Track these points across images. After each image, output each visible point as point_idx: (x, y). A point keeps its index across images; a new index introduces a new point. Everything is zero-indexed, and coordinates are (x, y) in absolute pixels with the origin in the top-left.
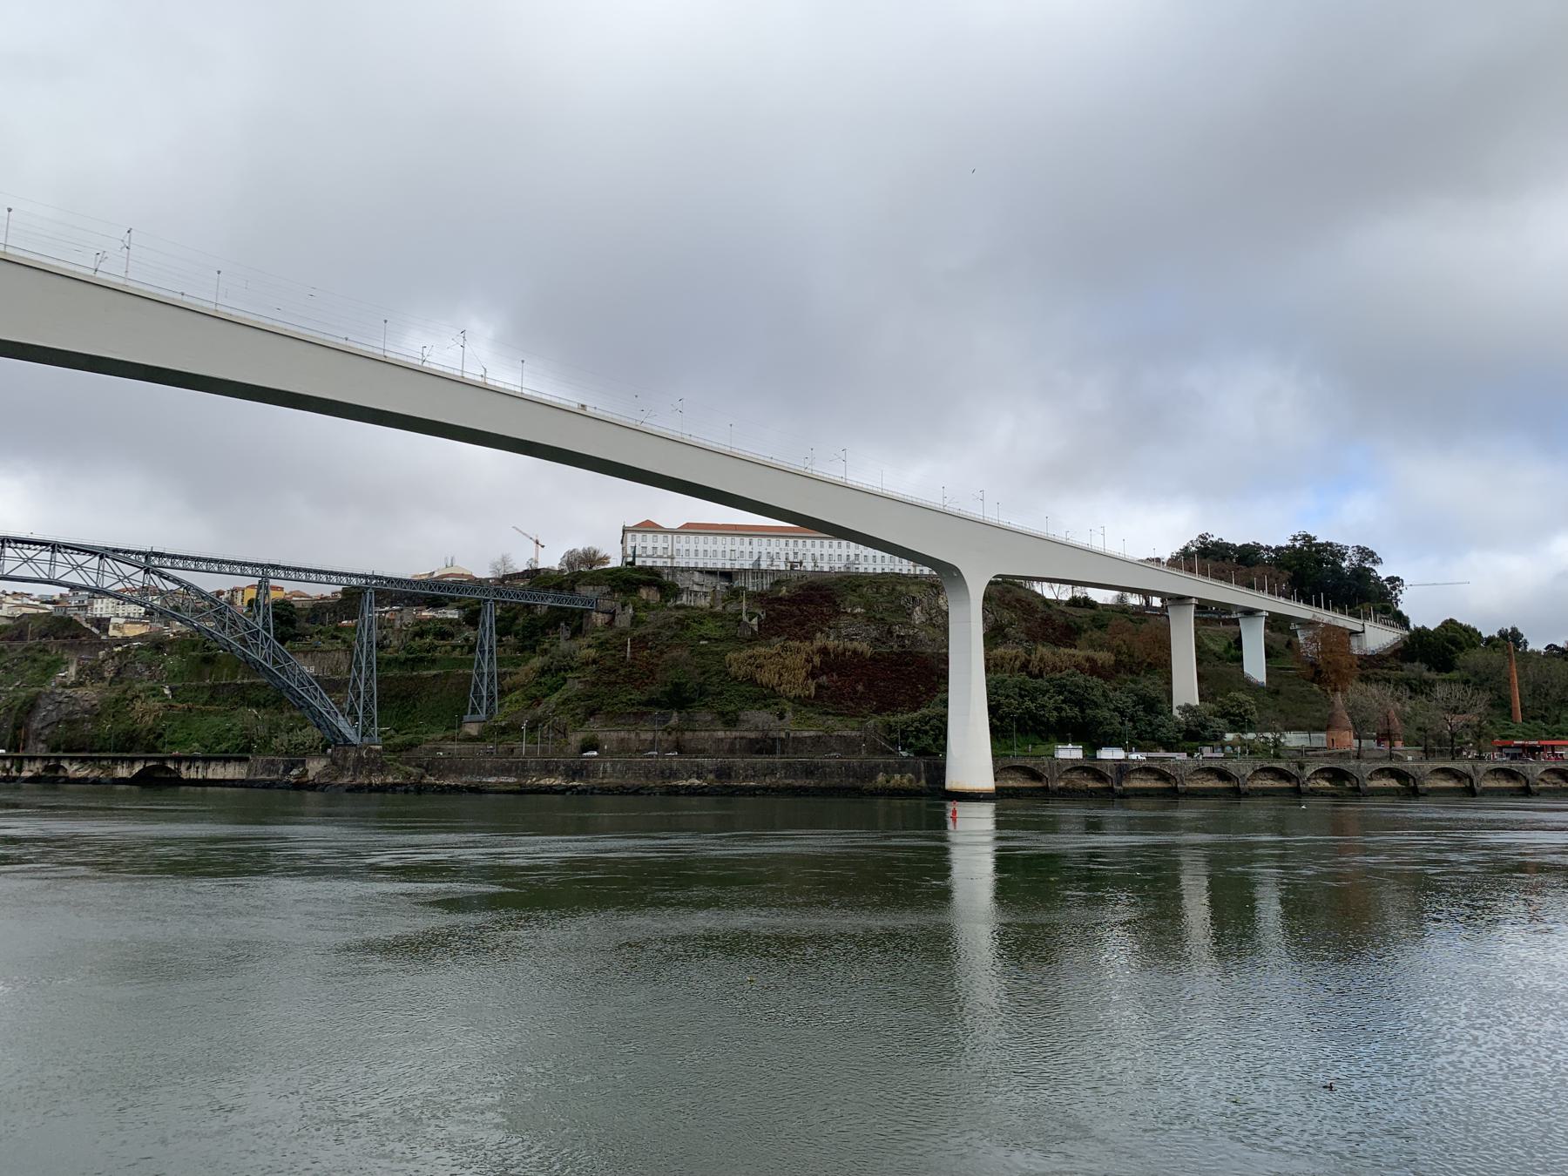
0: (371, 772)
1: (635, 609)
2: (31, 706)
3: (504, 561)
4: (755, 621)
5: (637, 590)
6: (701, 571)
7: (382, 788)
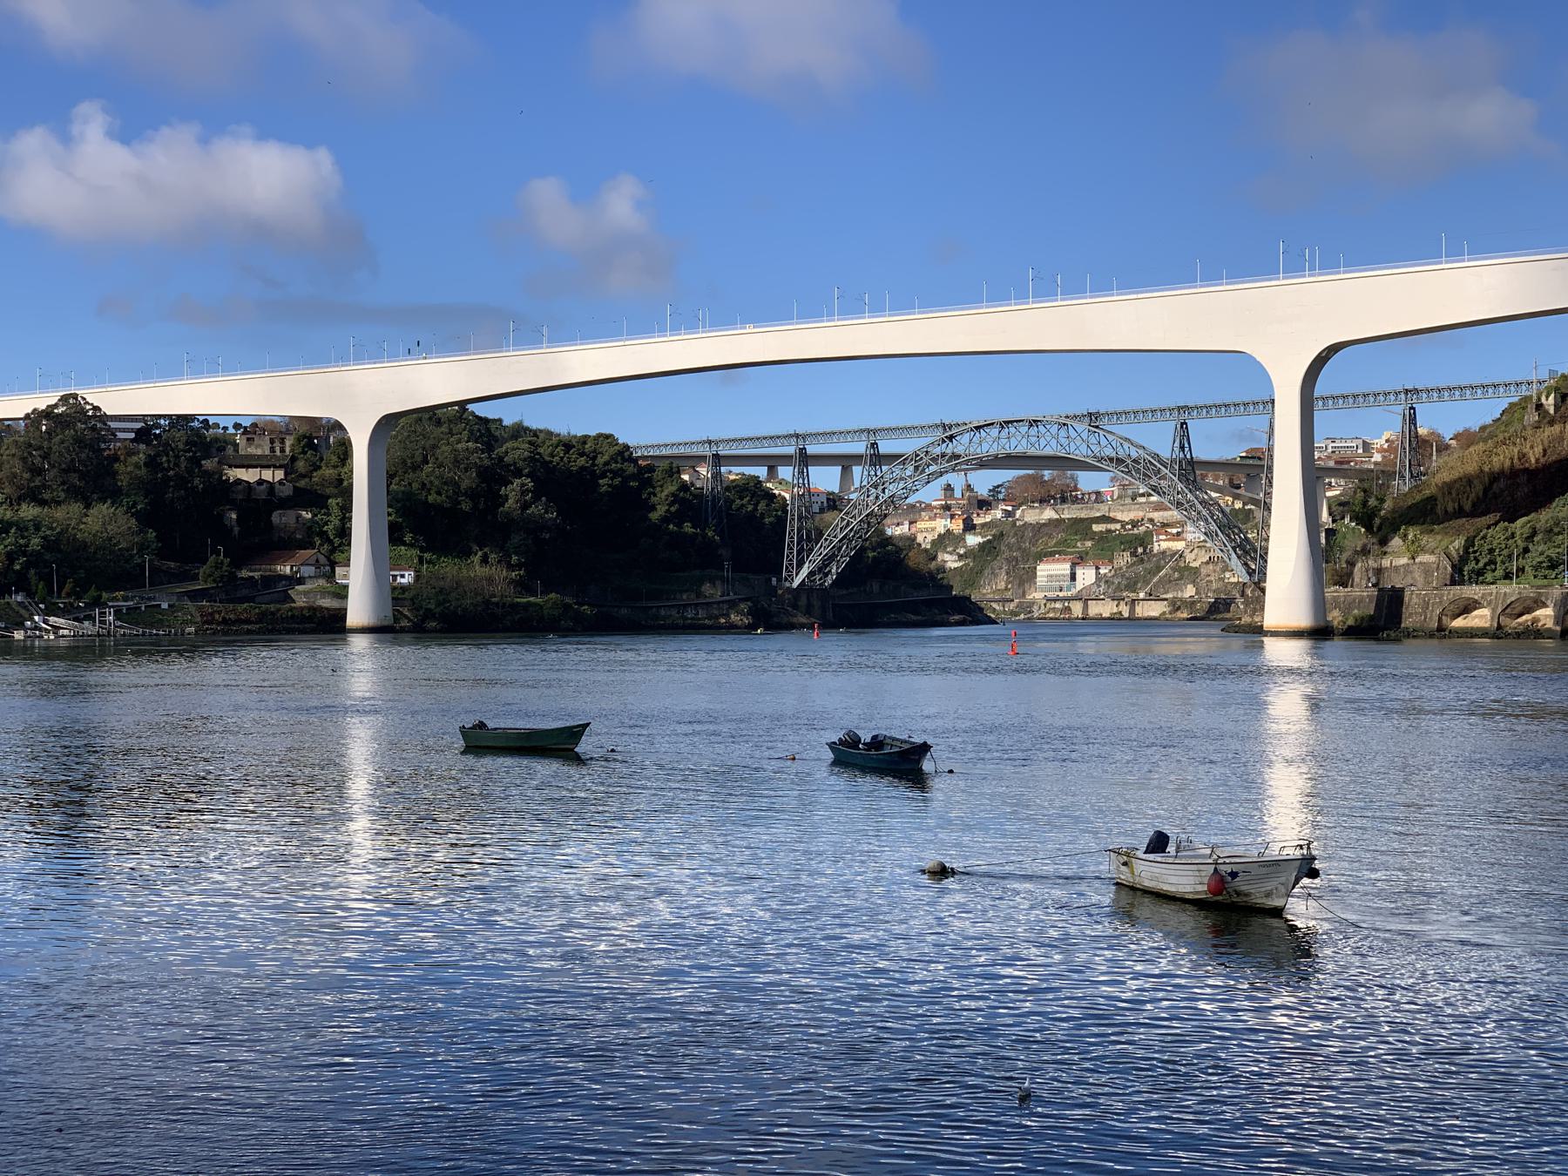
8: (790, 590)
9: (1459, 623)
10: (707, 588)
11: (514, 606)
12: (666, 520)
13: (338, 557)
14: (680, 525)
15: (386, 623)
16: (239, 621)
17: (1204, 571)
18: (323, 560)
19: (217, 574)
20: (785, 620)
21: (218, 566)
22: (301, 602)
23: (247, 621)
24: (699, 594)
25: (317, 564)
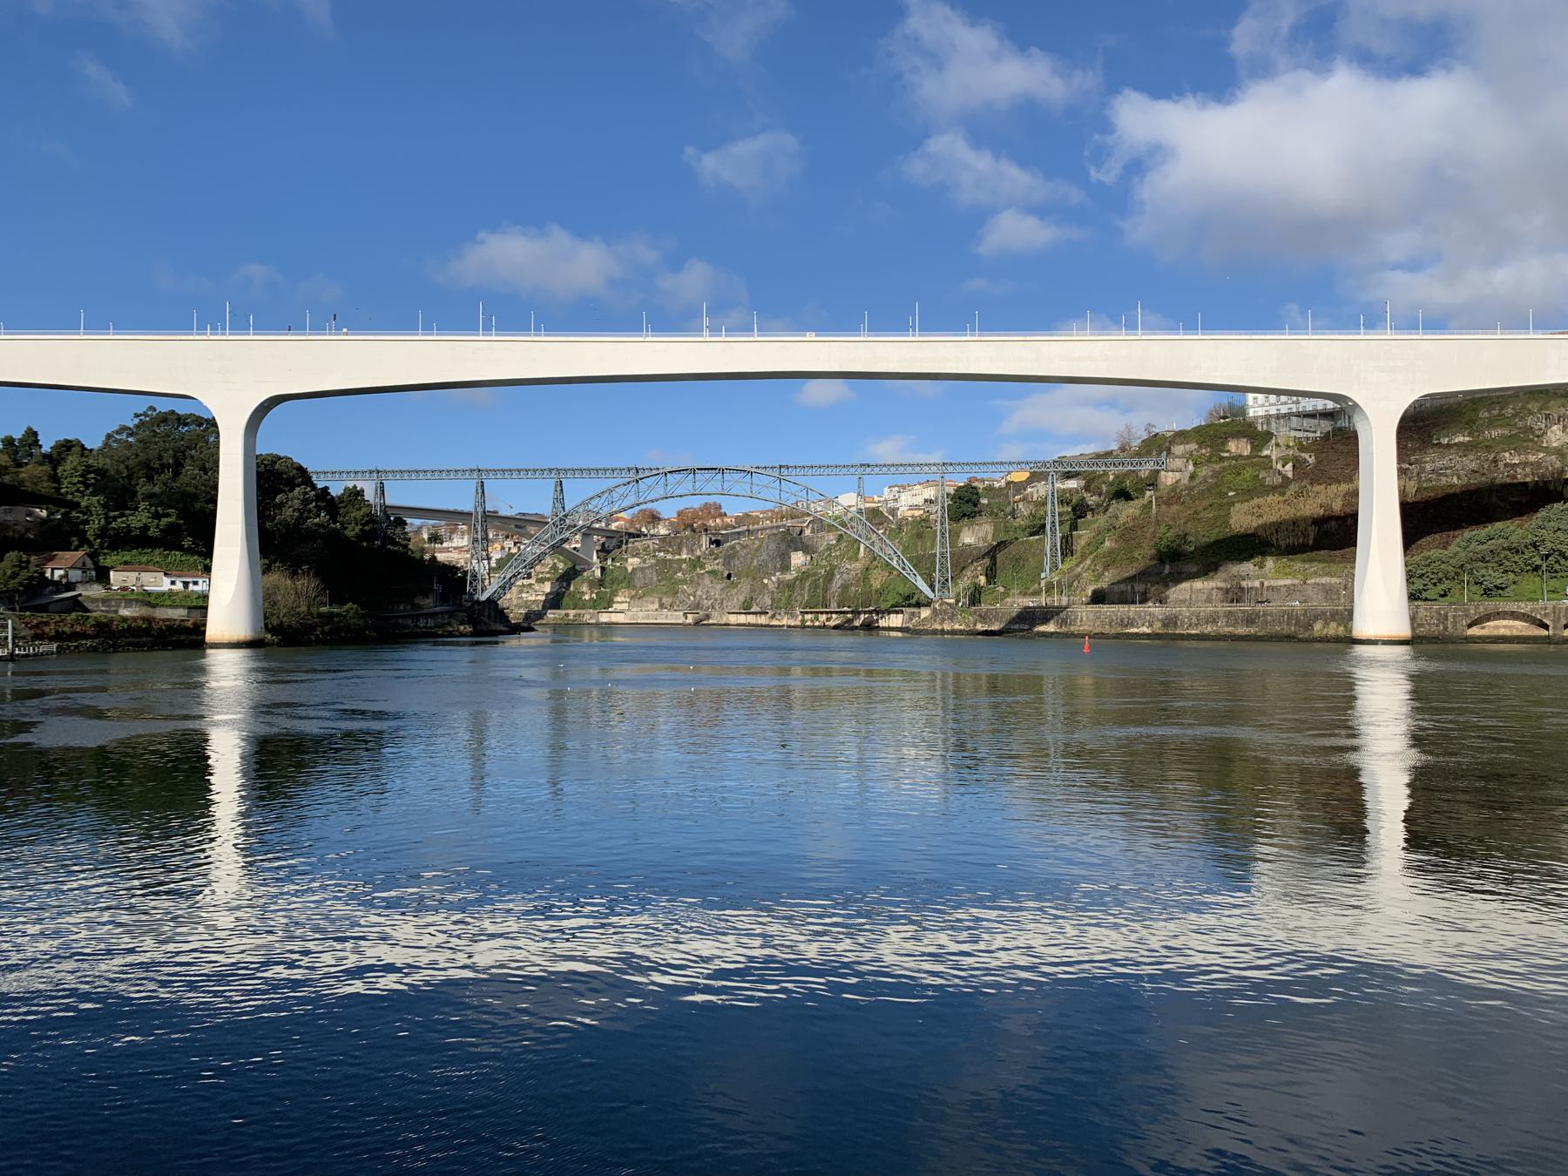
2: (830, 576)
3: (1128, 429)
4: (1289, 466)
5: (1224, 443)
6: (1298, 415)
7: (953, 632)
8: (478, 602)
9: (1475, 631)
10: (428, 603)
11: (320, 615)
12: (357, 536)
15: (262, 636)
16: (76, 636)
18: (89, 562)
19: (24, 574)
21: (23, 565)
22: (98, 613)
24: (420, 607)
25: (84, 568)
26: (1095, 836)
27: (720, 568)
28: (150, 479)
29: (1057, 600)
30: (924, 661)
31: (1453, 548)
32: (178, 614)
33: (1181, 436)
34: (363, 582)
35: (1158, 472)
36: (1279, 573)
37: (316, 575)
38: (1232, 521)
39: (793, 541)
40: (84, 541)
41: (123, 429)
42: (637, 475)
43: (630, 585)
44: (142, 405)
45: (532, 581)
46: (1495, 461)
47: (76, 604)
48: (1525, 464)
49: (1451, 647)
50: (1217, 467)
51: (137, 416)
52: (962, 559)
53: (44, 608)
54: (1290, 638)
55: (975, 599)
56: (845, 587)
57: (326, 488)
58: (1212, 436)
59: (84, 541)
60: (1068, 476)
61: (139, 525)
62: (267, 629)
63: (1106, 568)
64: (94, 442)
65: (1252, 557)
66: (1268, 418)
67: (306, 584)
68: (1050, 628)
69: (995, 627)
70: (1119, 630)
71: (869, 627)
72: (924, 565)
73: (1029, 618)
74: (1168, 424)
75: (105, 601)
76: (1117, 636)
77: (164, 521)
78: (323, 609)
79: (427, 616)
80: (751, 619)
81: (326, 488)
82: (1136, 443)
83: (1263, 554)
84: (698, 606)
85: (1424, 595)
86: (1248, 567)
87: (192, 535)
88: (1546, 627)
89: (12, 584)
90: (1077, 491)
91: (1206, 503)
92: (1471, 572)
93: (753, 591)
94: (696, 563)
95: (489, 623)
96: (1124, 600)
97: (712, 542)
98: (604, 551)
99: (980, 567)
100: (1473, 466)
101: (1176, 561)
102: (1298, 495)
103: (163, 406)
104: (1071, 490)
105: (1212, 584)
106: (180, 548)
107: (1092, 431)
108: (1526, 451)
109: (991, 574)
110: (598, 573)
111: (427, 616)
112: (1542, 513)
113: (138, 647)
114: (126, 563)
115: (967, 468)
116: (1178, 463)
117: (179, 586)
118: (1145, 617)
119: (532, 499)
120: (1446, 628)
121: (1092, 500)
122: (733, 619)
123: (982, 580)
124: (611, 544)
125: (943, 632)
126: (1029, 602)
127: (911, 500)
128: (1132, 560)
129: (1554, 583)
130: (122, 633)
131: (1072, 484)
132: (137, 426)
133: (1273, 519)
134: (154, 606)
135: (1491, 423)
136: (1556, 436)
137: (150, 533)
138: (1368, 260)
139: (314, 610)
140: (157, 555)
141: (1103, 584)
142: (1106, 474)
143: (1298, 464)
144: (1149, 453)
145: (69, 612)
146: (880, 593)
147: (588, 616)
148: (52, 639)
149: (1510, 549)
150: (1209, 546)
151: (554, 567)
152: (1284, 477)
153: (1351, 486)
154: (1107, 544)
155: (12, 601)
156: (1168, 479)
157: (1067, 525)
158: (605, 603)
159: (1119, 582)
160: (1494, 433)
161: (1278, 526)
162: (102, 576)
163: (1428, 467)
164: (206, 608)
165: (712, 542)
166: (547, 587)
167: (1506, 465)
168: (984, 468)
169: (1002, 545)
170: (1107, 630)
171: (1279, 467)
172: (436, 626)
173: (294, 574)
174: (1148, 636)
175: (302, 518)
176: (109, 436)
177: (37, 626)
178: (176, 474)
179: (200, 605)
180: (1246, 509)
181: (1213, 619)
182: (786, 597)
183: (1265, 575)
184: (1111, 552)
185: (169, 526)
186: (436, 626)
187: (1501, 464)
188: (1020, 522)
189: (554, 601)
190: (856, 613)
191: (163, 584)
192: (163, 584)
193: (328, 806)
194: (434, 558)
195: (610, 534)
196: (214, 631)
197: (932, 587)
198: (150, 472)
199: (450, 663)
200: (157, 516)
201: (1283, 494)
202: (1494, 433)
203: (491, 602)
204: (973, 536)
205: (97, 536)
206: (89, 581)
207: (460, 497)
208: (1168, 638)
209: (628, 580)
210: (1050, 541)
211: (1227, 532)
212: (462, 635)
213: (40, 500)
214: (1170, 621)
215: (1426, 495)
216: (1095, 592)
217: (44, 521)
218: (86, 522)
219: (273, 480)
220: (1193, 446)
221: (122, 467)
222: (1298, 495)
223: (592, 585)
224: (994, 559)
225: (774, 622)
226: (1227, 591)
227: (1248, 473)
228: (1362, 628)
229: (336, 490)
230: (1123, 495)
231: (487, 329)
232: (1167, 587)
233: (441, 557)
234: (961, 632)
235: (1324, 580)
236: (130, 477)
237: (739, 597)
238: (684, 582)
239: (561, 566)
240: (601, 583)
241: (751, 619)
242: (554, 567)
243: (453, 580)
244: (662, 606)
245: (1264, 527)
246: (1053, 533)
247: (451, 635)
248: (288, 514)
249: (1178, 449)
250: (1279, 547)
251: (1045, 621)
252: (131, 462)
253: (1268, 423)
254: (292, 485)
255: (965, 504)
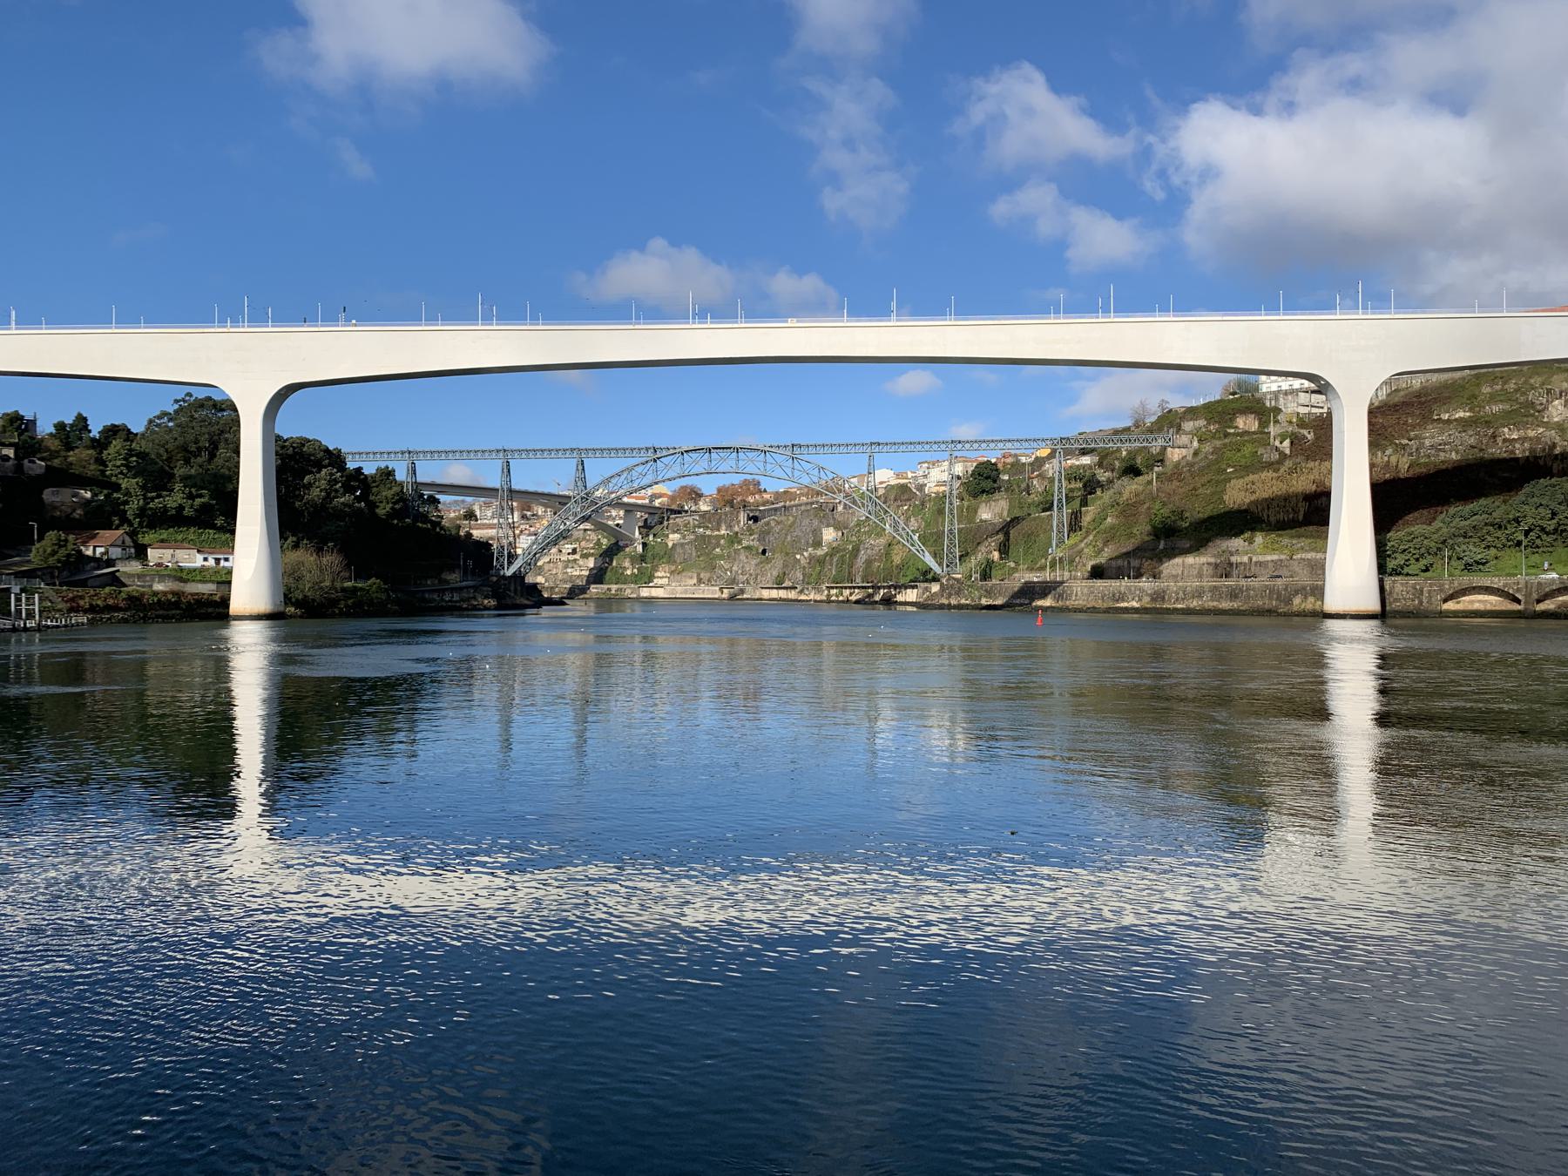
0: (950, 596)
1: (1200, 441)
2: (856, 550)
4: (1287, 443)
5: (1232, 420)
7: (960, 607)
10: (454, 577)
11: (344, 590)
12: (391, 515)
13: (145, 539)
14: (401, 519)
16: (109, 608)
17: (546, 567)
18: (128, 539)
19: (63, 552)
20: (509, 601)
21: (61, 544)
22: (134, 587)
23: (116, 608)
24: (447, 582)
25: (123, 546)
26: (1107, 803)
27: (756, 543)
28: (187, 462)
29: (1058, 575)
30: (937, 633)
31: (1437, 524)
32: (206, 588)
33: (1192, 412)
34: (389, 558)
35: (1165, 448)
36: (1267, 548)
37: (340, 551)
38: (1226, 498)
39: (825, 513)
40: (124, 520)
41: (164, 414)
42: (655, 454)
43: (671, 561)
44: (180, 393)
45: (577, 556)
46: (1494, 437)
47: (114, 580)
48: (1523, 440)
49: (1426, 622)
50: (1218, 443)
51: (176, 401)
52: (972, 538)
53: (83, 584)
54: (1270, 612)
55: (986, 576)
56: (869, 562)
57: (359, 470)
58: (1220, 413)
59: (124, 520)
60: (1084, 452)
61: (175, 505)
62: (287, 599)
63: (1106, 543)
64: (137, 427)
65: (1242, 533)
66: (1276, 394)
67: (331, 559)
68: (1047, 602)
69: (999, 602)
70: (1111, 604)
71: (888, 602)
72: (932, 540)
73: (1030, 592)
74: (1177, 403)
75: (140, 576)
76: (1108, 610)
77: (198, 501)
78: (348, 584)
79: (453, 590)
80: (782, 594)
81: (359, 470)
82: (1150, 420)
83: (1253, 530)
84: (733, 581)
85: (1406, 570)
86: (1237, 543)
87: (216, 515)
88: (1518, 602)
89: (51, 561)
90: (1090, 467)
91: (1205, 479)
92: (1452, 548)
93: (785, 566)
94: (734, 539)
95: (519, 597)
96: (1118, 574)
97: (749, 519)
98: (646, 527)
99: (993, 542)
100: (1472, 441)
101: (1171, 537)
102: (1291, 471)
103: (200, 394)
104: (1084, 466)
105: (1203, 559)
106: (213, 527)
107: (1101, 410)
108: (1525, 426)
109: (1004, 549)
110: (640, 549)
111: (453, 590)
112: (1527, 489)
113: (166, 619)
114: (162, 541)
115: (1001, 445)
116: (1184, 439)
117: (211, 562)
118: (1135, 592)
119: (555, 477)
120: (1421, 603)
121: (1103, 476)
122: (766, 594)
123: (996, 555)
124: (653, 520)
125: (949, 607)
126: (1035, 577)
127: (938, 477)
128: (1130, 535)
129: (1535, 559)
130: (152, 606)
131: (1086, 460)
132: (176, 412)
133: (1265, 495)
134: (186, 581)
135: (1493, 398)
136: (1557, 411)
137: (185, 513)
138: (1338, 246)
139: (338, 585)
140: (192, 533)
141: (1102, 560)
142: (1119, 450)
143: (1296, 440)
144: (1160, 430)
145: (103, 587)
146: (900, 568)
147: (629, 591)
148: (85, 611)
149: (1493, 525)
150: (1204, 521)
151: (598, 543)
152: (1282, 454)
153: (1381, 458)
154: (1109, 520)
155: (53, 577)
156: (1174, 455)
157: (1078, 501)
158: (646, 578)
159: (1117, 558)
160: (1495, 409)
161: (1269, 502)
162: (141, 553)
163: (1427, 442)
164: (230, 583)
165: (749, 519)
166: (591, 563)
167: (1505, 440)
168: (1017, 445)
169: (1015, 521)
170: (1099, 604)
171: (1277, 443)
172: (462, 600)
173: (319, 550)
174: (1136, 611)
175: (329, 495)
176: (150, 421)
177: (72, 600)
178: (212, 456)
179: (225, 580)
180: (1222, 490)
181: (1199, 594)
182: (816, 572)
183: (1253, 551)
184: (1112, 527)
185: (203, 505)
186: (462, 600)
187: (1499, 440)
188: (1034, 498)
189: (597, 576)
190: (876, 588)
191: (197, 560)
192: (197, 560)
193: (362, 768)
194: (469, 535)
195: (650, 510)
196: (237, 604)
197: (940, 564)
198: (188, 455)
199: (483, 639)
200: (191, 497)
201: (1276, 471)
202: (1495, 409)
203: (518, 577)
204: (990, 512)
205: (137, 516)
206: (129, 558)
207: (491, 477)
208: (1156, 613)
209: (668, 555)
210: (1059, 517)
211: (1221, 508)
212: (486, 608)
213: (84, 482)
214: (1159, 596)
215: (1418, 470)
216: (1093, 567)
217: (88, 502)
218: (126, 503)
219: (294, 464)
220: (1201, 422)
221: (162, 451)
222: (1291, 471)
223: (633, 560)
224: (1007, 535)
225: (803, 597)
226: (1216, 566)
227: (1248, 449)
228: (1332, 603)
229: (369, 469)
230: (1132, 471)
231: (487, 319)
232: (1161, 562)
233: (476, 534)
234: (966, 607)
235: (1309, 556)
236: (169, 459)
237: (773, 572)
238: (721, 557)
239: (605, 541)
240: (643, 558)
241: (782, 594)
242: (598, 543)
243: (481, 552)
244: (700, 581)
245: (1255, 503)
246: (1060, 509)
247: (475, 608)
248: (316, 494)
249: (1188, 426)
250: (1269, 523)
251: (1044, 595)
252: (170, 446)
253: (1277, 399)
254: (319, 466)
255: (985, 480)
